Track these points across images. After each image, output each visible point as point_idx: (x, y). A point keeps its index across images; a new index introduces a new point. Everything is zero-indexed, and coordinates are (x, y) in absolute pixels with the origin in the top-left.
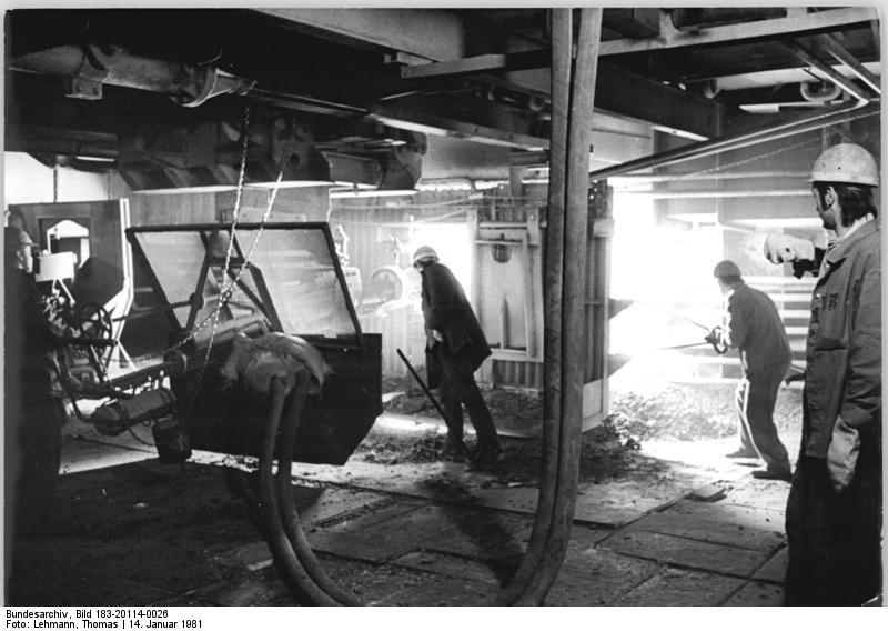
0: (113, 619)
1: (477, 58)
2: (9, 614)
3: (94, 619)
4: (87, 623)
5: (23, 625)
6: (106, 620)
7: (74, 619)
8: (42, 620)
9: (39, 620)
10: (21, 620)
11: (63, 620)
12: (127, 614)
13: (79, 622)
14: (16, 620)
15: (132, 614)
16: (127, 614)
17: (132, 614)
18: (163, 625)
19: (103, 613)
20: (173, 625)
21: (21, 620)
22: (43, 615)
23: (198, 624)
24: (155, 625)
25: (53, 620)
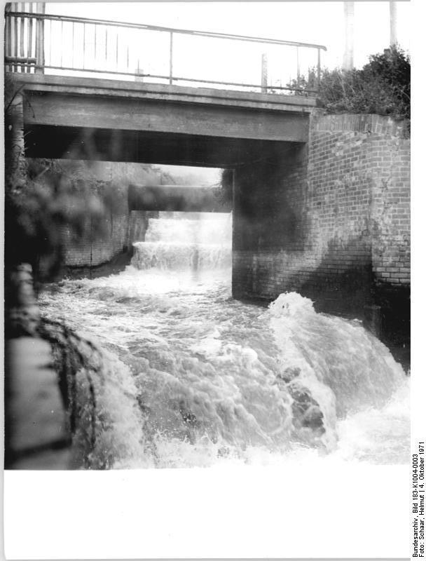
2: (415, 556)
5: (423, 546)
10: (419, 548)
14: (419, 551)
21: (419, 548)
22: (416, 534)
23: (421, 445)
25: (419, 525)
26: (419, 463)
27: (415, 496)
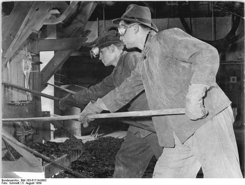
1: (106, 117)
5: (6, 183)
10: (6, 182)
14: (4, 182)
15: (36, 180)
17: (36, 180)
20: (34, 183)
21: (6, 182)
22: (12, 181)
25: (15, 182)
26: (31, 182)
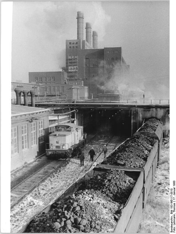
0: (173, 204)
2: (171, 232)
3: (173, 209)
4: (174, 211)
5: (175, 228)
6: (173, 206)
7: (173, 214)
8: (173, 223)
9: (173, 224)
10: (173, 228)
11: (173, 217)
12: (171, 199)
13: (174, 213)
14: (173, 230)
16: (171, 199)
18: (174, 191)
19: (171, 207)
21: (173, 228)
24: (174, 193)
25: (173, 220)
27: (171, 207)
